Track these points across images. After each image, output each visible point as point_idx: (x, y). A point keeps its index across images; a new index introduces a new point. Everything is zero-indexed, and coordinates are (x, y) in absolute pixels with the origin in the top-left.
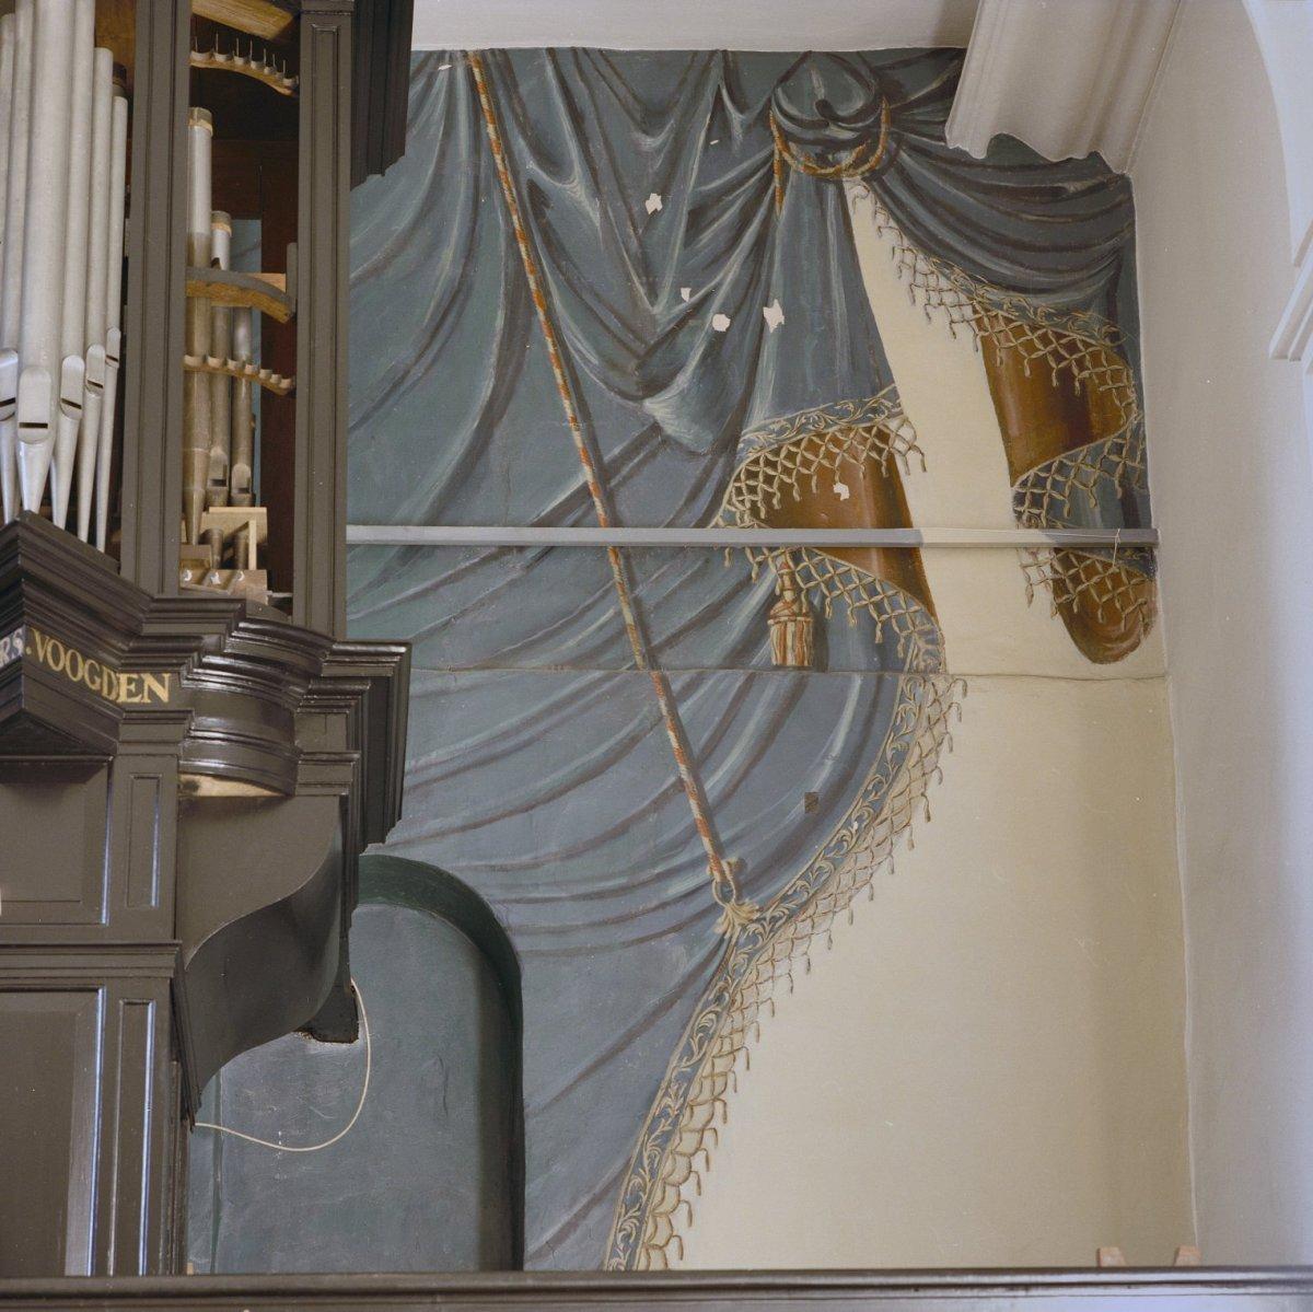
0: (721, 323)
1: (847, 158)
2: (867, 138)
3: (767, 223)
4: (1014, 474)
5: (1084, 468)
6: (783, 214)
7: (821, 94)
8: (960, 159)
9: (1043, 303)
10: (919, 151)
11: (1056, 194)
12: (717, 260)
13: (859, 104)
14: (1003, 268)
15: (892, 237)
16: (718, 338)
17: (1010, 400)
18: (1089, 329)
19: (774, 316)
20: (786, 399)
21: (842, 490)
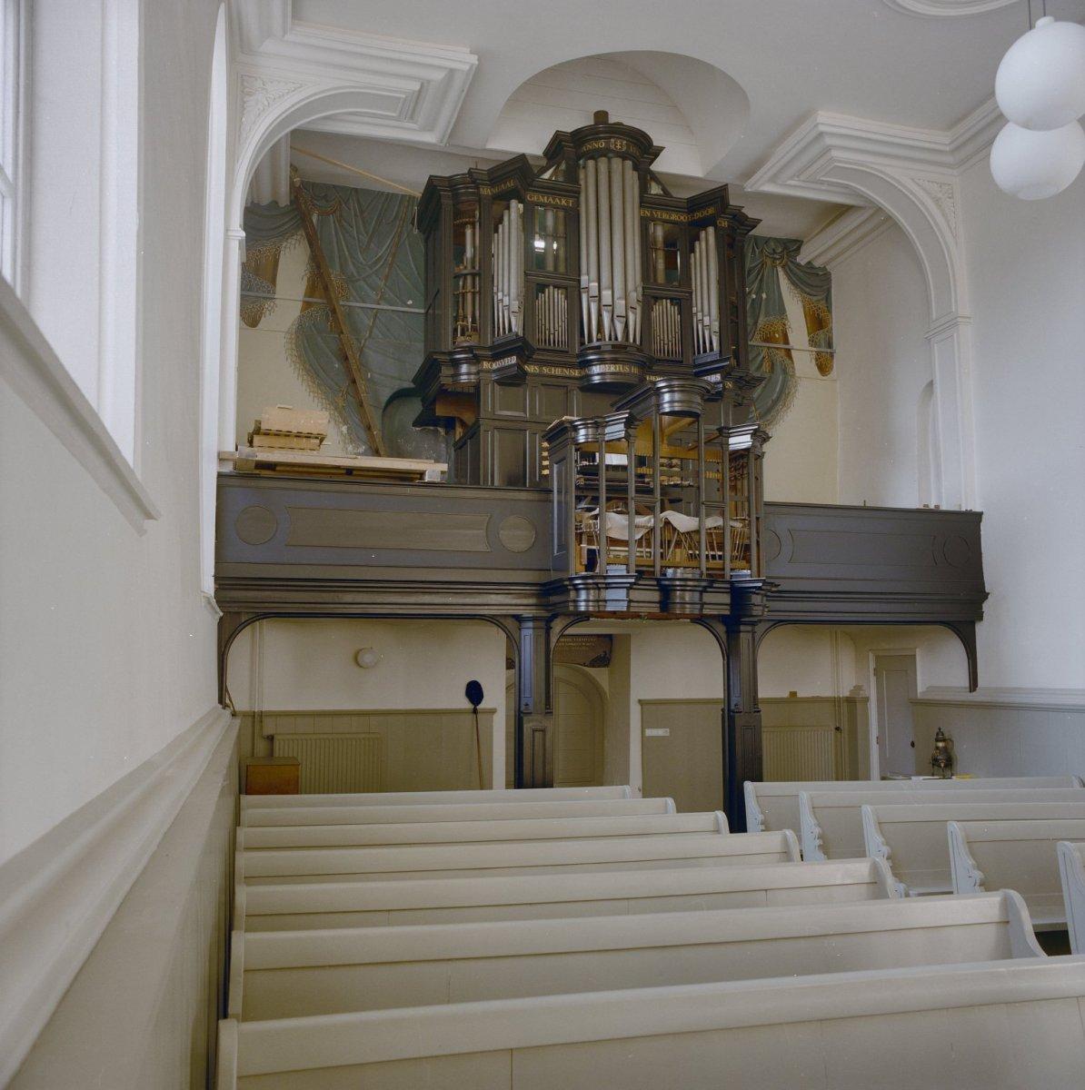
0: (754, 296)
1: (778, 262)
2: (782, 258)
3: (763, 275)
4: (809, 334)
5: (821, 335)
6: (765, 274)
7: (774, 247)
8: (798, 265)
9: (815, 298)
10: (792, 262)
11: (818, 274)
12: (753, 282)
13: (780, 250)
14: (807, 290)
15: (786, 281)
16: (753, 300)
17: (808, 319)
18: (822, 305)
19: (764, 296)
20: (767, 314)
21: (777, 335)
